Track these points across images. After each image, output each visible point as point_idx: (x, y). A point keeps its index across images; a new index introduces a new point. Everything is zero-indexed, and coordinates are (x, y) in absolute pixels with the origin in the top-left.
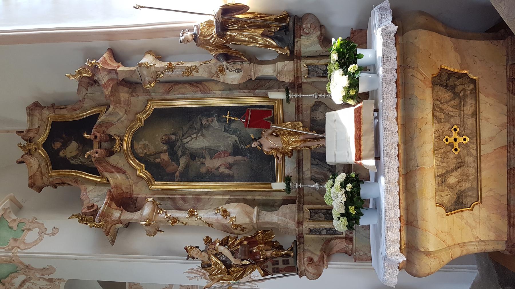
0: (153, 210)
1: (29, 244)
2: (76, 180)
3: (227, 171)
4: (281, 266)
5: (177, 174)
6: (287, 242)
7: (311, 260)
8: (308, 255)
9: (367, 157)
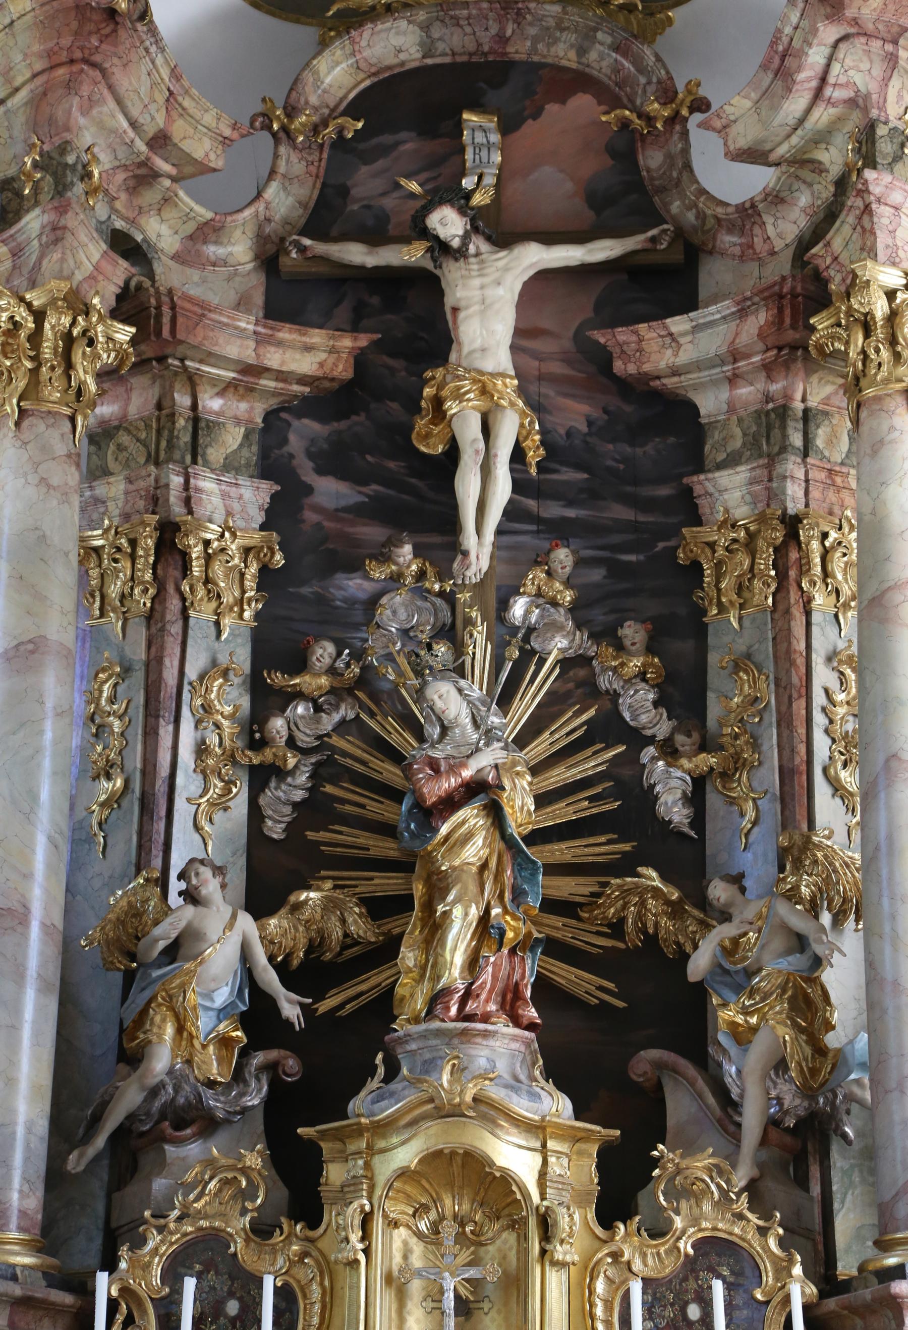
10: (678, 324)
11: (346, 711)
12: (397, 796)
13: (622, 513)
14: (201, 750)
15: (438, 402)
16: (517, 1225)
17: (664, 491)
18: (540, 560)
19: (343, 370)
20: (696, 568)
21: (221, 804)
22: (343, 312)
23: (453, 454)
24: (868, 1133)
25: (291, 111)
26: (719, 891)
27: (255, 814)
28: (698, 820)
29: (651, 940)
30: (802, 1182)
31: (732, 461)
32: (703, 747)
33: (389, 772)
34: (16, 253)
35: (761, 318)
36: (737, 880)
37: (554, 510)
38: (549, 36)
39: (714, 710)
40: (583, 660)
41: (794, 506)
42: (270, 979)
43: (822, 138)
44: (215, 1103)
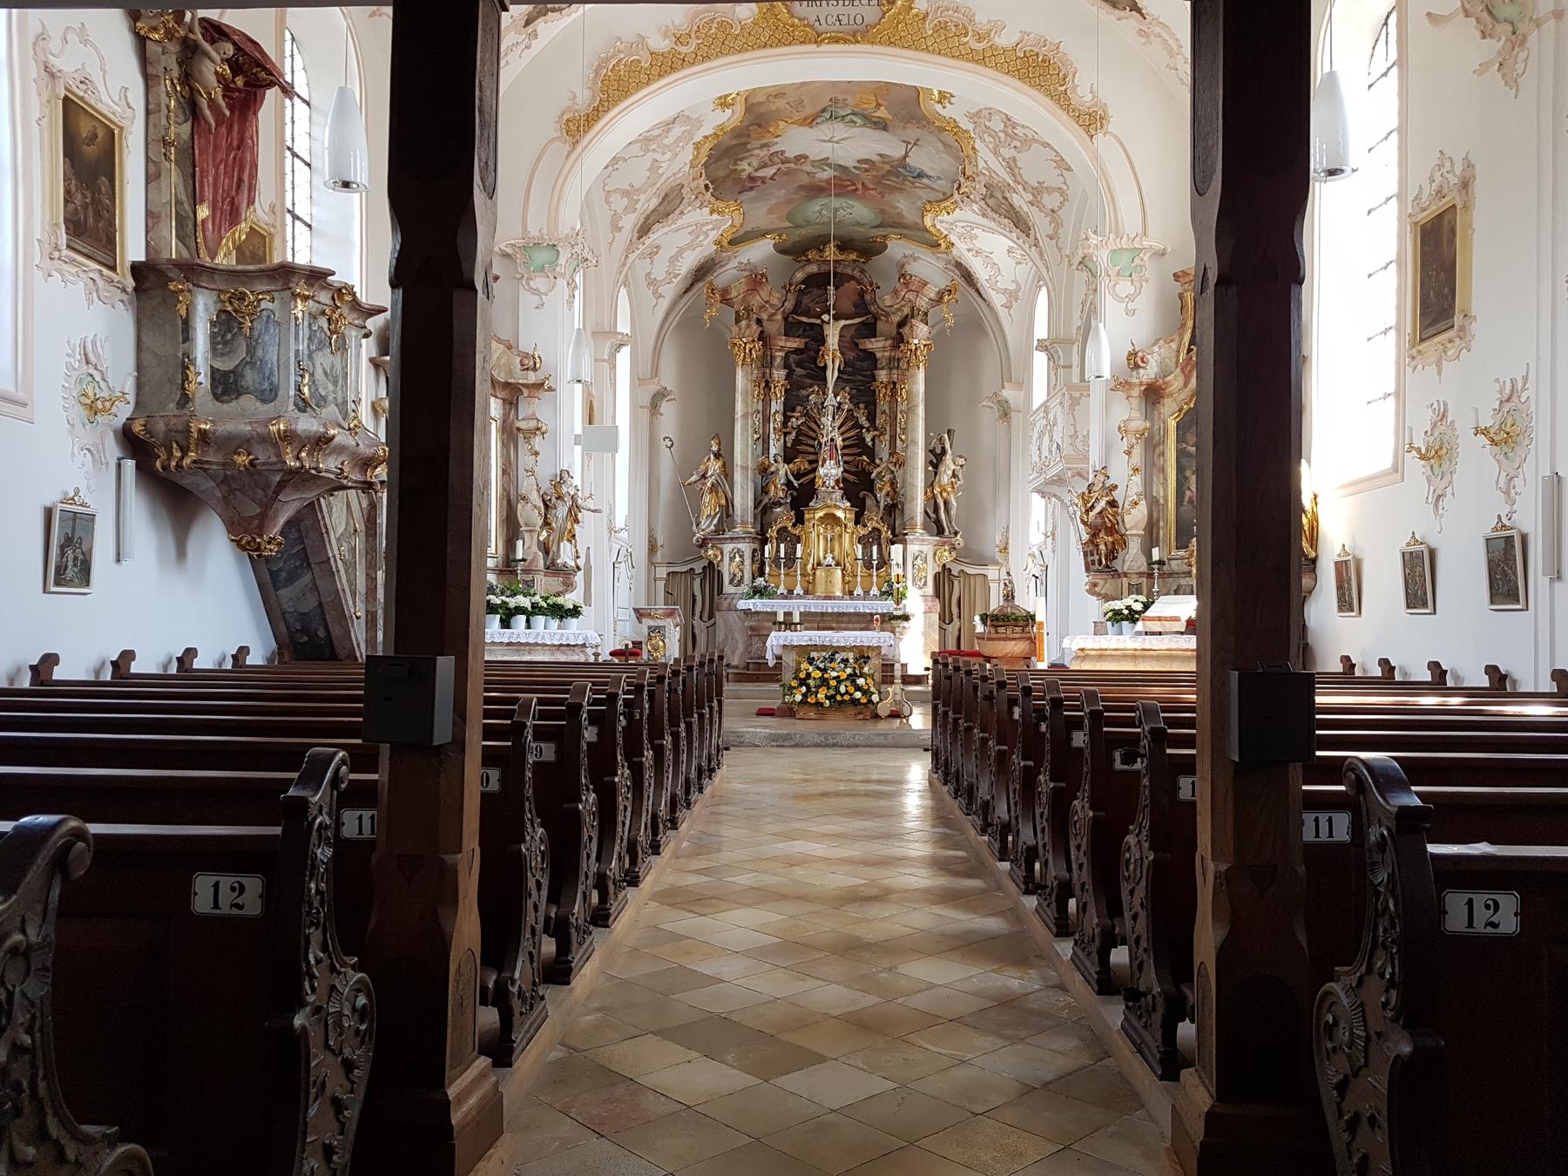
0: (1137, 432)
1: (1114, 290)
2: (1183, 325)
3: (1187, 499)
4: (1090, 558)
5: (1184, 445)
6: (1117, 564)
7: (1095, 585)
8: (1101, 582)
9: (1144, 626)
10: (873, 340)
11: (803, 420)
12: (815, 439)
13: (860, 378)
14: (774, 428)
15: (823, 355)
16: (841, 526)
17: (869, 373)
18: (843, 389)
19: (802, 346)
20: (875, 391)
21: (778, 440)
22: (801, 332)
23: (825, 367)
24: (903, 507)
25: (791, 285)
26: (877, 461)
27: (785, 441)
28: (873, 445)
29: (864, 469)
30: (890, 516)
31: (882, 368)
32: (876, 429)
33: (814, 435)
34: (740, 329)
35: (890, 342)
36: (881, 459)
37: (845, 377)
38: (846, 267)
39: (877, 422)
40: (851, 410)
41: (895, 380)
42: (791, 478)
43: (904, 306)
44: (782, 501)
